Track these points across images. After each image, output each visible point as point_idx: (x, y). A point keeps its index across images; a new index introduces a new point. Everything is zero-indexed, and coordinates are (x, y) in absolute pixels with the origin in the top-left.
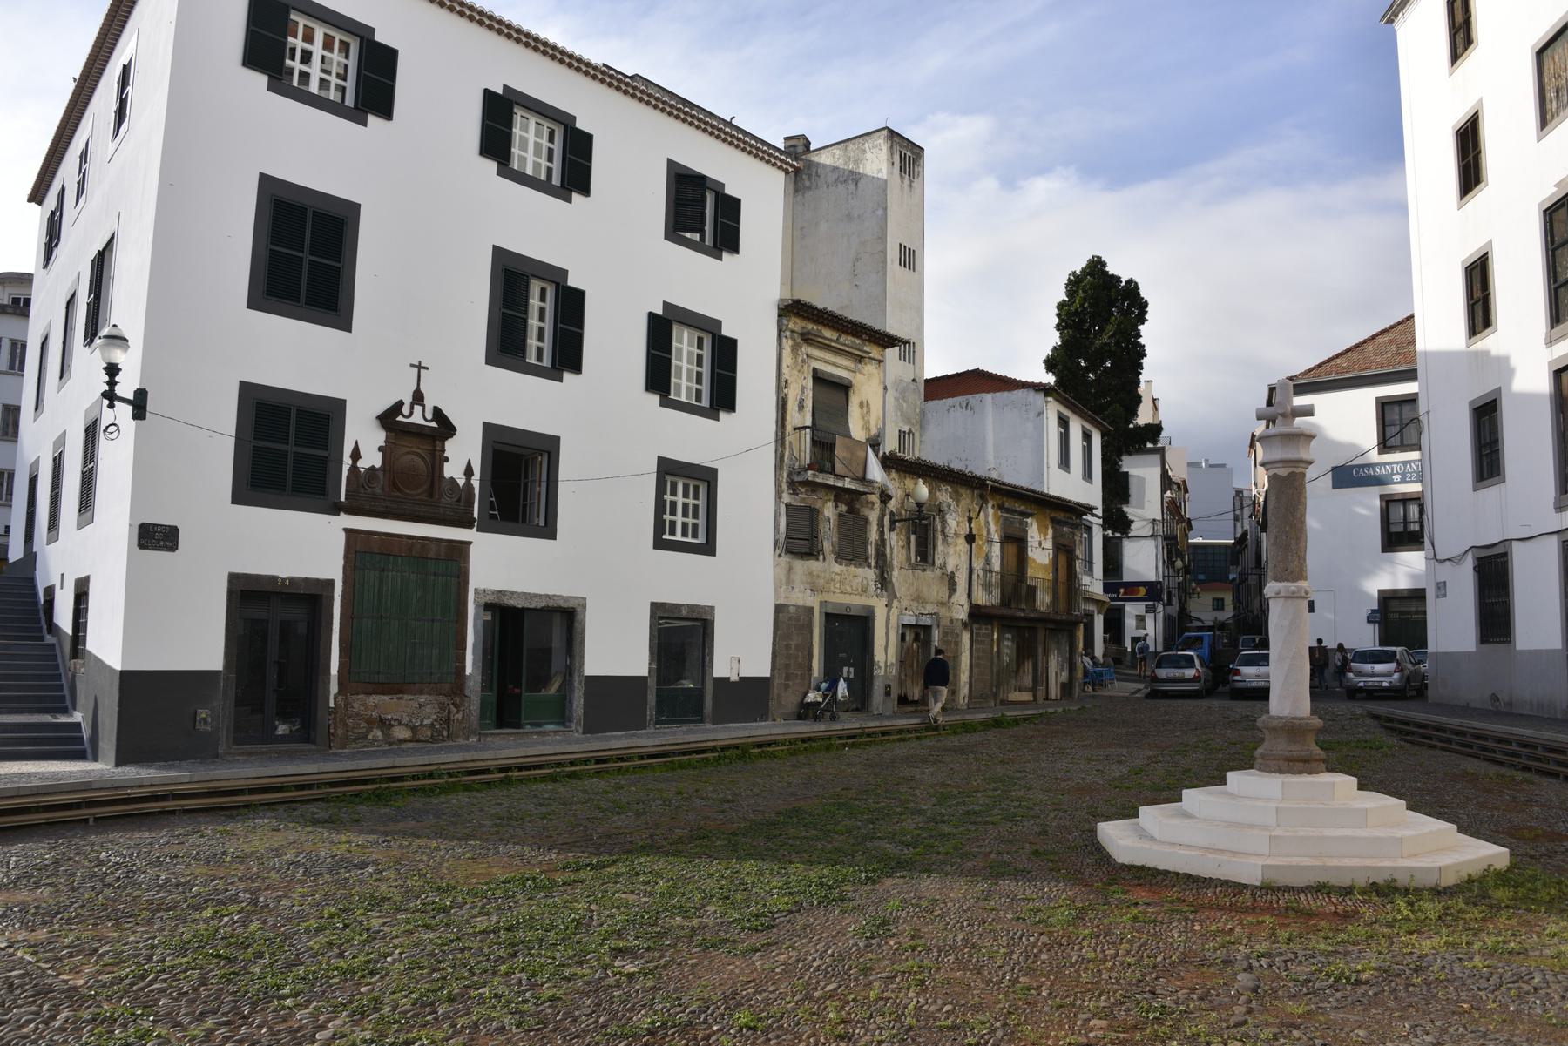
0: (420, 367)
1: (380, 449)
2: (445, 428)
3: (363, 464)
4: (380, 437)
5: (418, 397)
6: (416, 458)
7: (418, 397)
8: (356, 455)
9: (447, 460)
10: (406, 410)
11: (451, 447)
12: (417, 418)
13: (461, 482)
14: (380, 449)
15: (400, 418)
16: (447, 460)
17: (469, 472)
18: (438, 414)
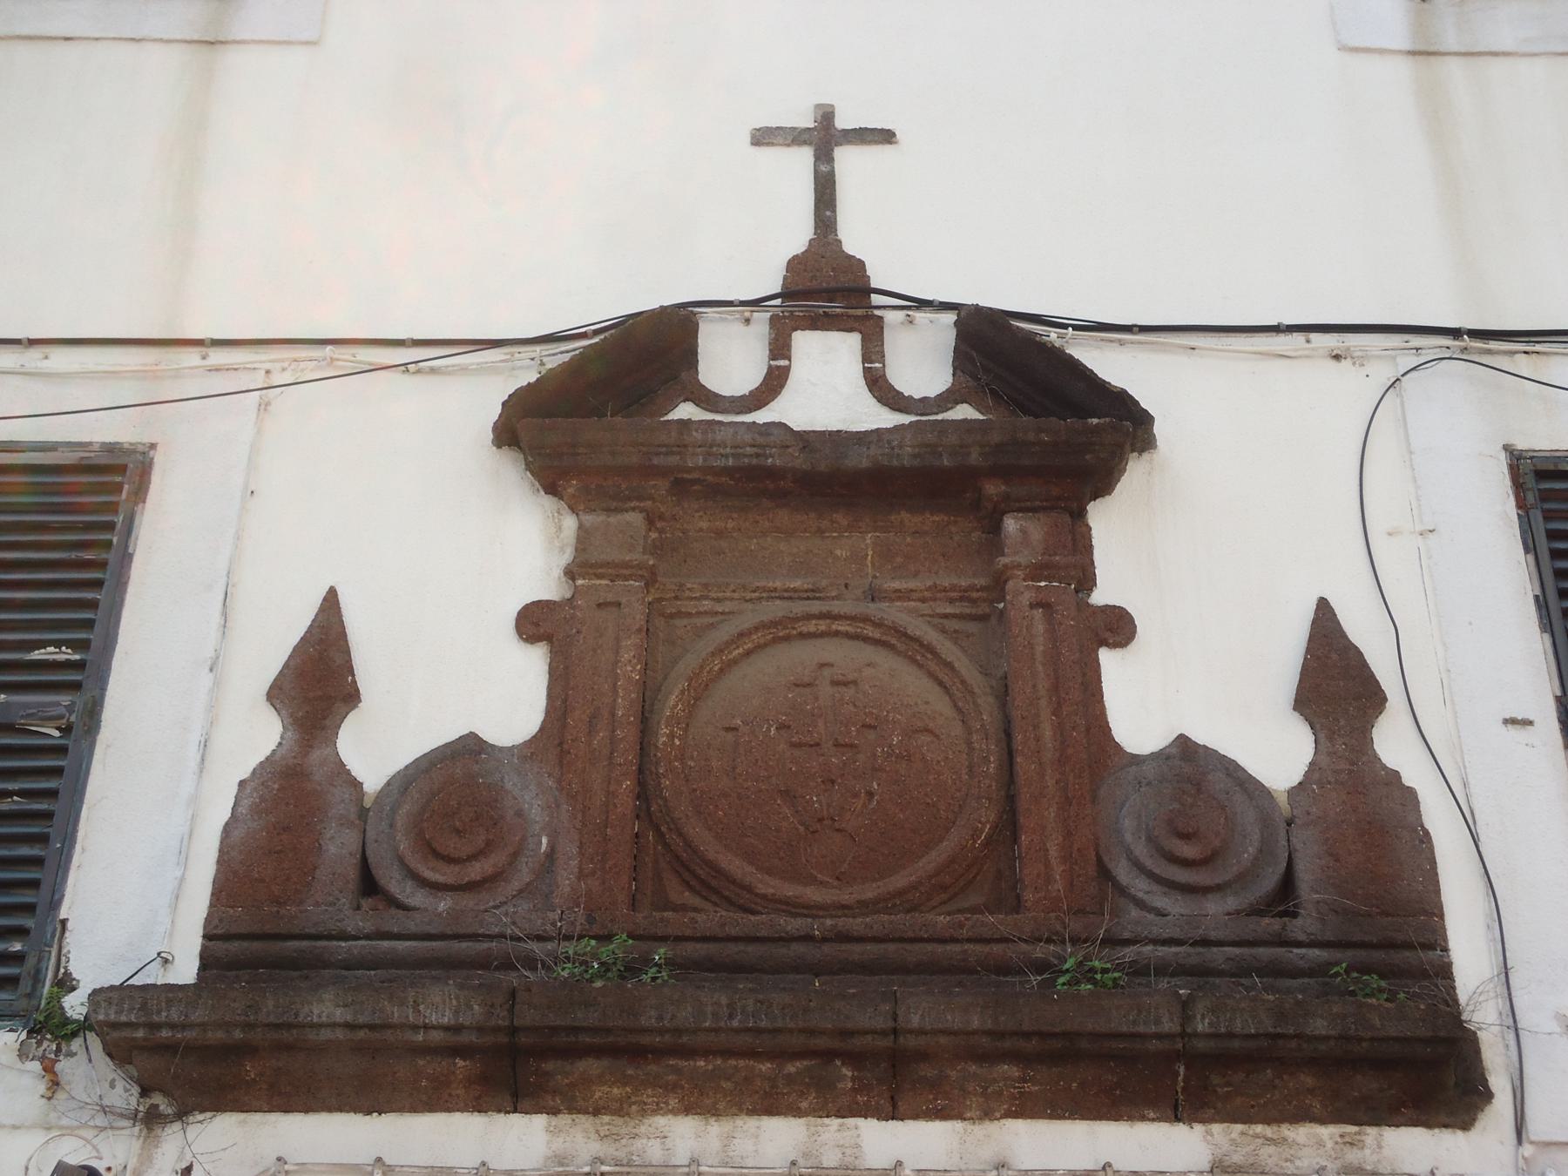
0: (825, 137)
1: (534, 623)
2: (1041, 423)
3: (376, 748)
4: (524, 545)
5: (828, 290)
6: (843, 655)
7: (828, 290)
8: (319, 680)
9: (1117, 627)
10: (729, 360)
11: (1130, 543)
12: (826, 391)
13: (1278, 754)
14: (534, 623)
15: (686, 411)
16: (1117, 627)
17: (1337, 684)
18: (998, 350)
